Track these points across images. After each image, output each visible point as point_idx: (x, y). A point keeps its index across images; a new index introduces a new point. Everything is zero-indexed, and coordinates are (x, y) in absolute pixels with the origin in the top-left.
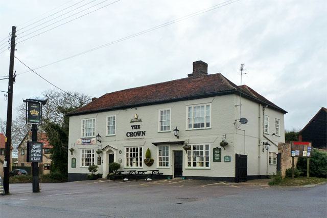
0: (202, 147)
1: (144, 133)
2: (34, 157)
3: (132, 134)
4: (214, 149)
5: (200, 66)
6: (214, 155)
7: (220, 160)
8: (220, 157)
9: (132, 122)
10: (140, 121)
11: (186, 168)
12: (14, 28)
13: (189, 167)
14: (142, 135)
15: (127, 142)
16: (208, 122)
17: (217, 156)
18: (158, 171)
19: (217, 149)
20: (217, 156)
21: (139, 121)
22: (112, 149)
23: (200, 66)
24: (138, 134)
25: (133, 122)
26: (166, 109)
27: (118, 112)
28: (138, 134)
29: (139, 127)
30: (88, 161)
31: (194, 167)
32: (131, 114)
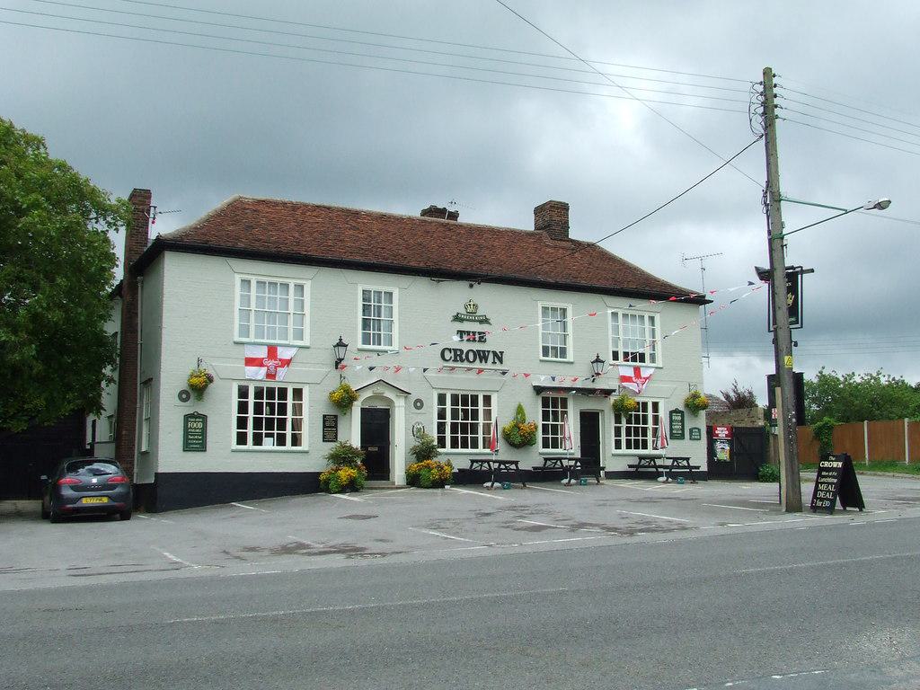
0: (645, 405)
1: (499, 357)
2: (30, 394)
3: (459, 355)
4: (671, 412)
5: (553, 216)
6: (671, 425)
7: (682, 437)
8: (683, 429)
9: (457, 318)
10: (485, 321)
11: (234, 448)
12: (768, 73)
13: (619, 451)
14: (494, 363)
15: (444, 375)
16: (615, 349)
17: (677, 426)
18: (516, 463)
19: (676, 411)
20: (677, 426)
21: (481, 322)
22: (389, 394)
23: (553, 216)
24: (482, 356)
25: (462, 320)
26: (383, 289)
27: (405, 281)
28: (482, 356)
29: (482, 339)
30: (637, 434)
31: (295, 448)
32: (455, 296)
